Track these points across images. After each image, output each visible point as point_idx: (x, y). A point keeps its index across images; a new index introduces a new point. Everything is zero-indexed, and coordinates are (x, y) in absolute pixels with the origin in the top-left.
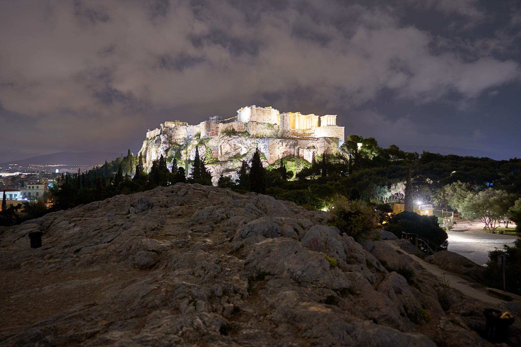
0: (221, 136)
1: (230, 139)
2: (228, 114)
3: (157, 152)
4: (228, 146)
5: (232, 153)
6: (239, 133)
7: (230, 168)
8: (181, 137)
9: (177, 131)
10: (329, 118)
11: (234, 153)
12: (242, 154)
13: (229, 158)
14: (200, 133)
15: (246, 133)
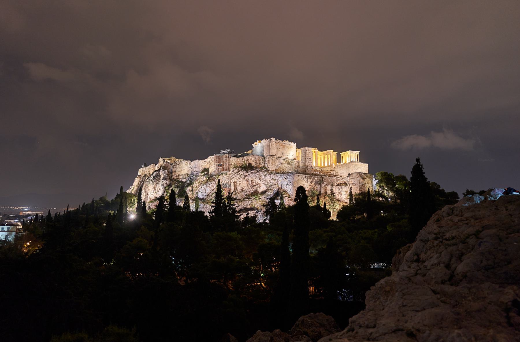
0: (235, 171)
1: (247, 174)
2: (242, 148)
3: (155, 189)
4: (244, 181)
5: (249, 190)
6: (257, 168)
7: (249, 207)
8: (184, 173)
9: (178, 166)
10: (352, 154)
11: (251, 190)
12: (261, 190)
13: (246, 195)
14: (209, 169)
15: (264, 169)
